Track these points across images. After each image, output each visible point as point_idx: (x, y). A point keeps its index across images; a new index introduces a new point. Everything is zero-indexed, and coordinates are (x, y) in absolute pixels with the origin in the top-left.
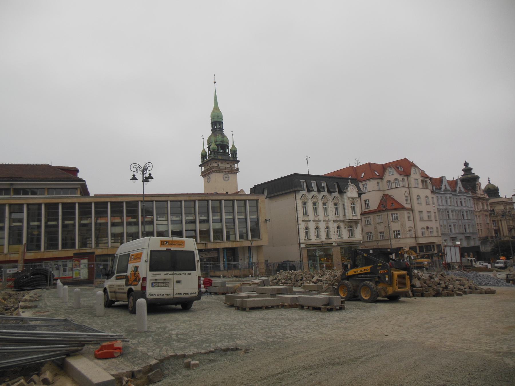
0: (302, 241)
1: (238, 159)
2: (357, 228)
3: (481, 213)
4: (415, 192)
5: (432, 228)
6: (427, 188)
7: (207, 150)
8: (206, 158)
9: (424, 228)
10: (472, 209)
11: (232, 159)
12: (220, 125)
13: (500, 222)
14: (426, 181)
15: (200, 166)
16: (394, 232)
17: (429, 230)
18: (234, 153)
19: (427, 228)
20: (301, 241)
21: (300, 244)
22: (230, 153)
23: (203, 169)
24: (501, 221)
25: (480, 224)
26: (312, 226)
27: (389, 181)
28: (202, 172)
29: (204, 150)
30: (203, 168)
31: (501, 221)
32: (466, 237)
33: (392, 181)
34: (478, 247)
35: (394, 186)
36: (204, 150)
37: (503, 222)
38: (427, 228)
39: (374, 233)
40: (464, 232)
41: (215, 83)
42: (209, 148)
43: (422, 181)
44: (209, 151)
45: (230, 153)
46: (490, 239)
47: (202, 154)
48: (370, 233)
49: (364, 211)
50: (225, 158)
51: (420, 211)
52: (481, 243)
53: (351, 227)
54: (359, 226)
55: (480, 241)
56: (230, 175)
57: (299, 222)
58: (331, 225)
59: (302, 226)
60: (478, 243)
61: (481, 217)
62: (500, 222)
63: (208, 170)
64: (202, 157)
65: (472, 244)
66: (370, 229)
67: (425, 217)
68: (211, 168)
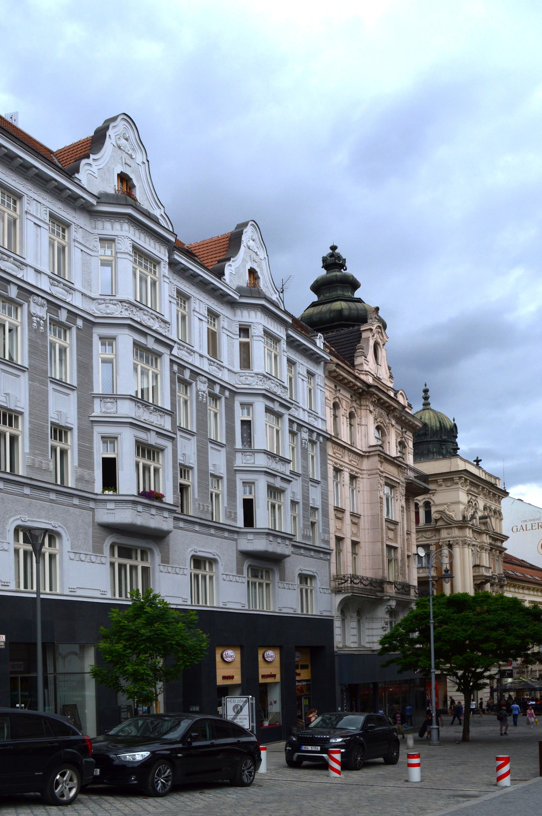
3: (366, 464)
10: (319, 424)
13: (446, 551)
24: (450, 546)
25: (355, 516)
31: (450, 546)
32: (246, 555)
34: (324, 625)
37: (457, 550)
40: (240, 522)
46: (391, 591)
52: (345, 608)
55: (339, 598)
60: (323, 604)
61: (363, 483)
62: (446, 551)
65: (284, 601)
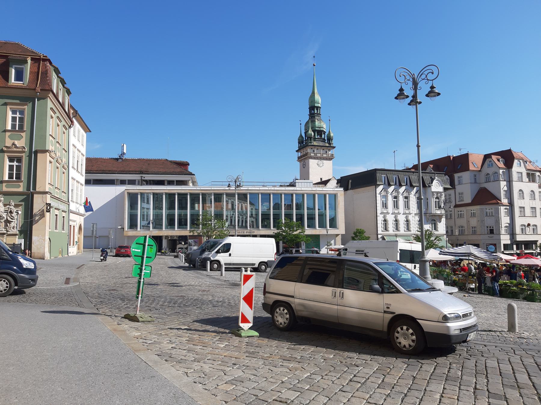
0: (380, 232)
1: (334, 145)
2: (440, 222)
4: (517, 186)
5: (536, 226)
6: (534, 181)
7: (303, 135)
8: (303, 143)
9: (525, 225)
11: (327, 145)
12: (317, 110)
14: (533, 175)
15: (297, 151)
16: (487, 227)
17: (531, 228)
18: (330, 139)
19: (529, 225)
20: (379, 232)
21: (377, 235)
22: (326, 139)
23: (300, 154)
26: (391, 219)
27: (488, 174)
28: (299, 158)
29: (301, 136)
30: (299, 153)
33: (491, 174)
35: (492, 178)
36: (301, 136)
38: (529, 225)
39: (466, 227)
41: (314, 65)
42: (305, 133)
43: (528, 174)
44: (305, 136)
45: (326, 139)
47: (298, 140)
48: (462, 227)
49: (458, 203)
50: (321, 144)
51: (520, 207)
53: (434, 221)
54: (443, 220)
56: (325, 161)
57: (378, 214)
58: (410, 218)
59: (380, 218)
63: (304, 156)
64: (299, 143)
66: (462, 222)
67: (528, 212)
68: (306, 154)
